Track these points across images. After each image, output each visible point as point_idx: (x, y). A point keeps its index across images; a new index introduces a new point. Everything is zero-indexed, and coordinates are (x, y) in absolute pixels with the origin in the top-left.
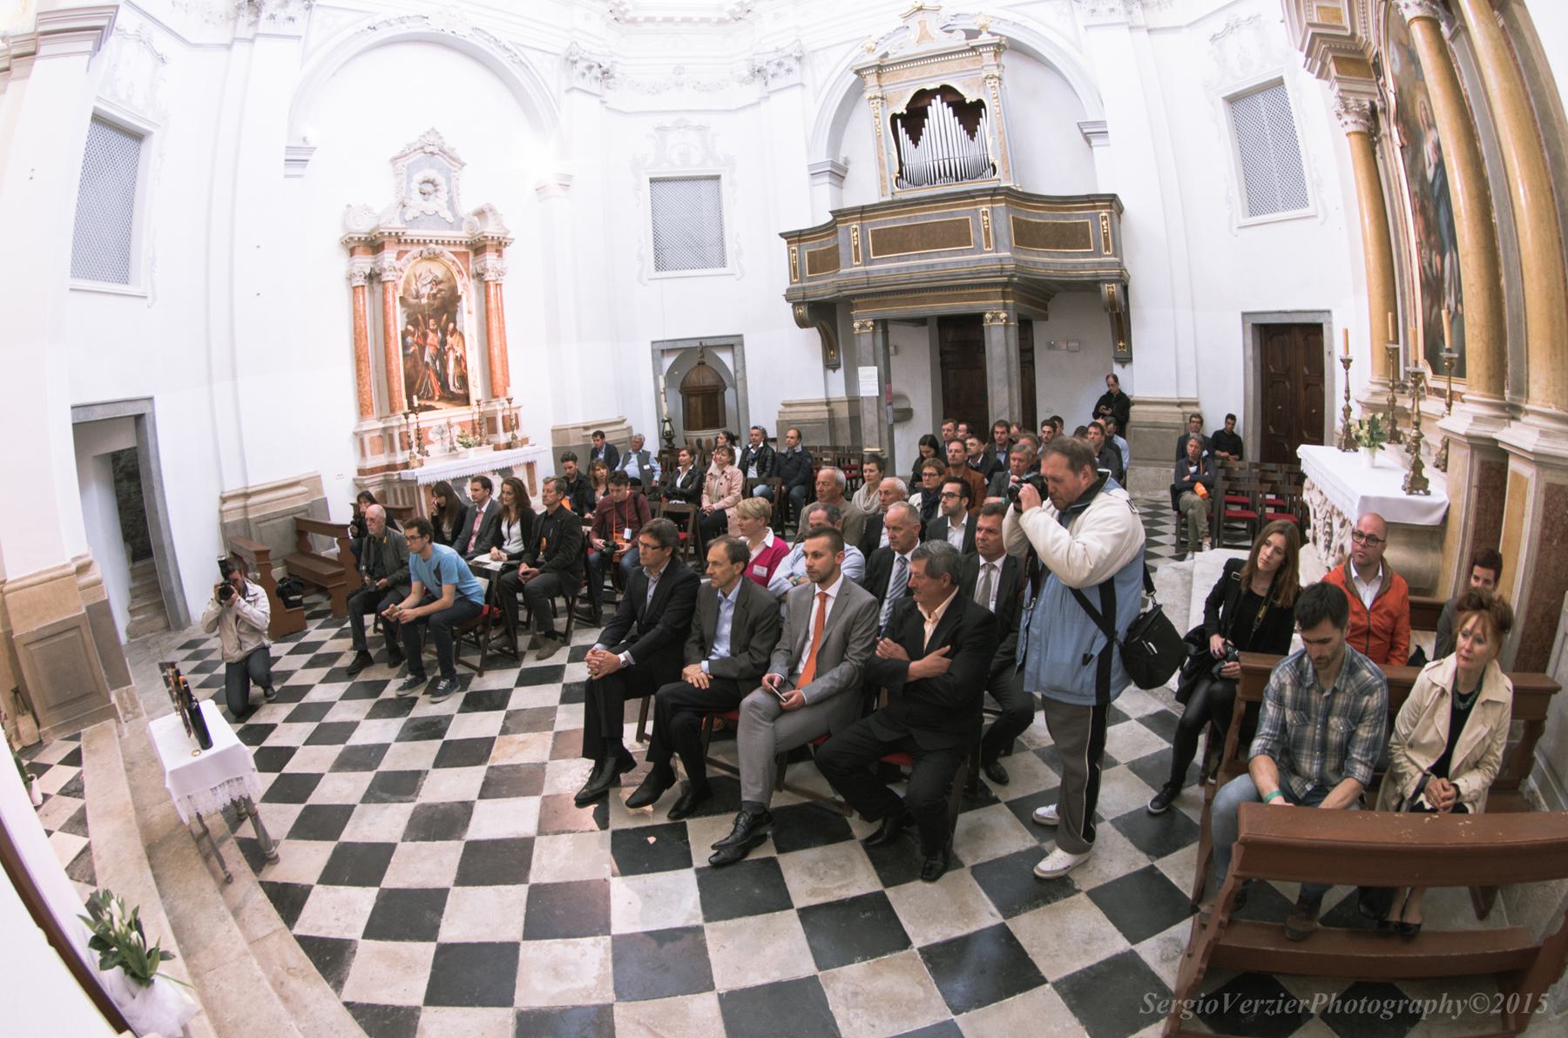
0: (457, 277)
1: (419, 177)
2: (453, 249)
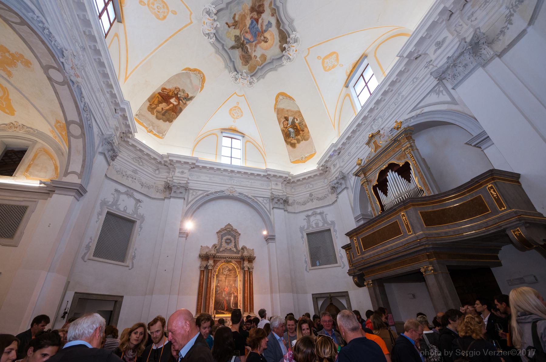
1: (225, 238)
2: (236, 260)
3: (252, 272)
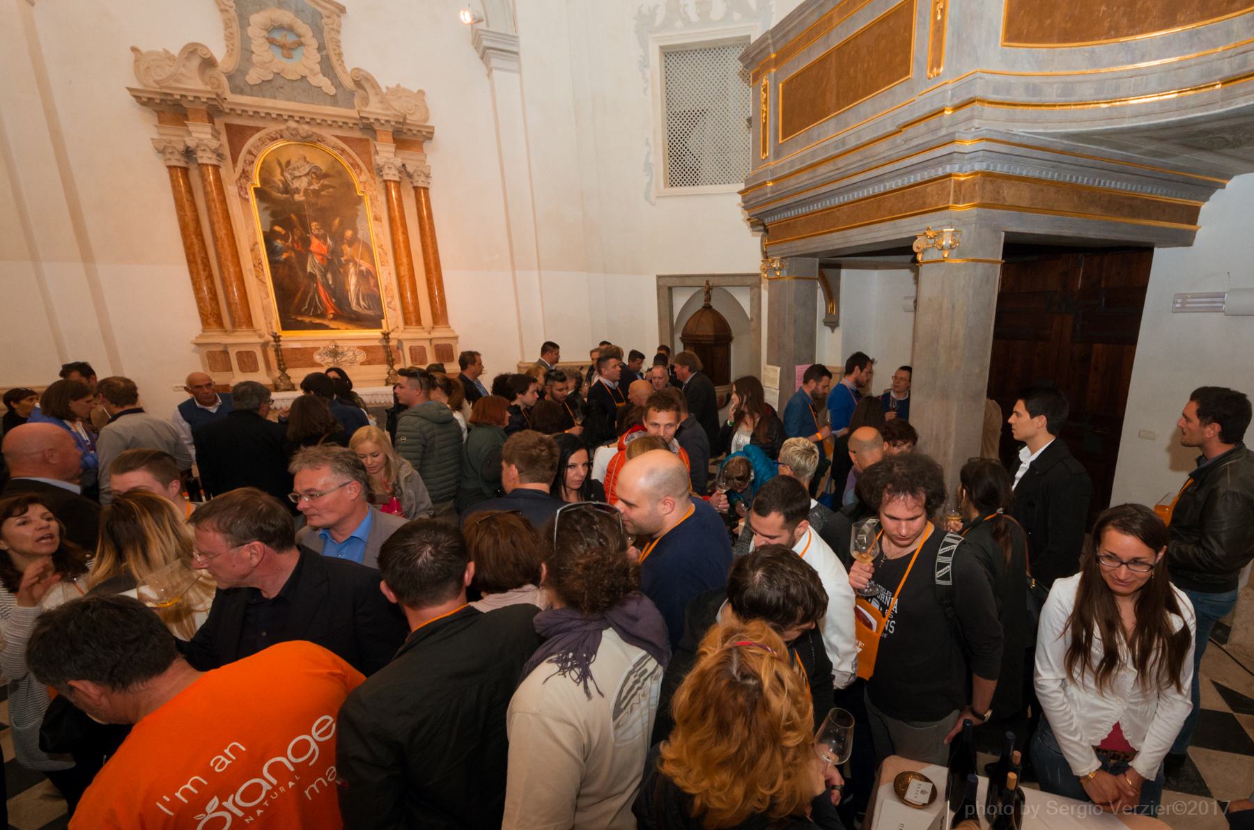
0: (353, 174)
3: (426, 189)
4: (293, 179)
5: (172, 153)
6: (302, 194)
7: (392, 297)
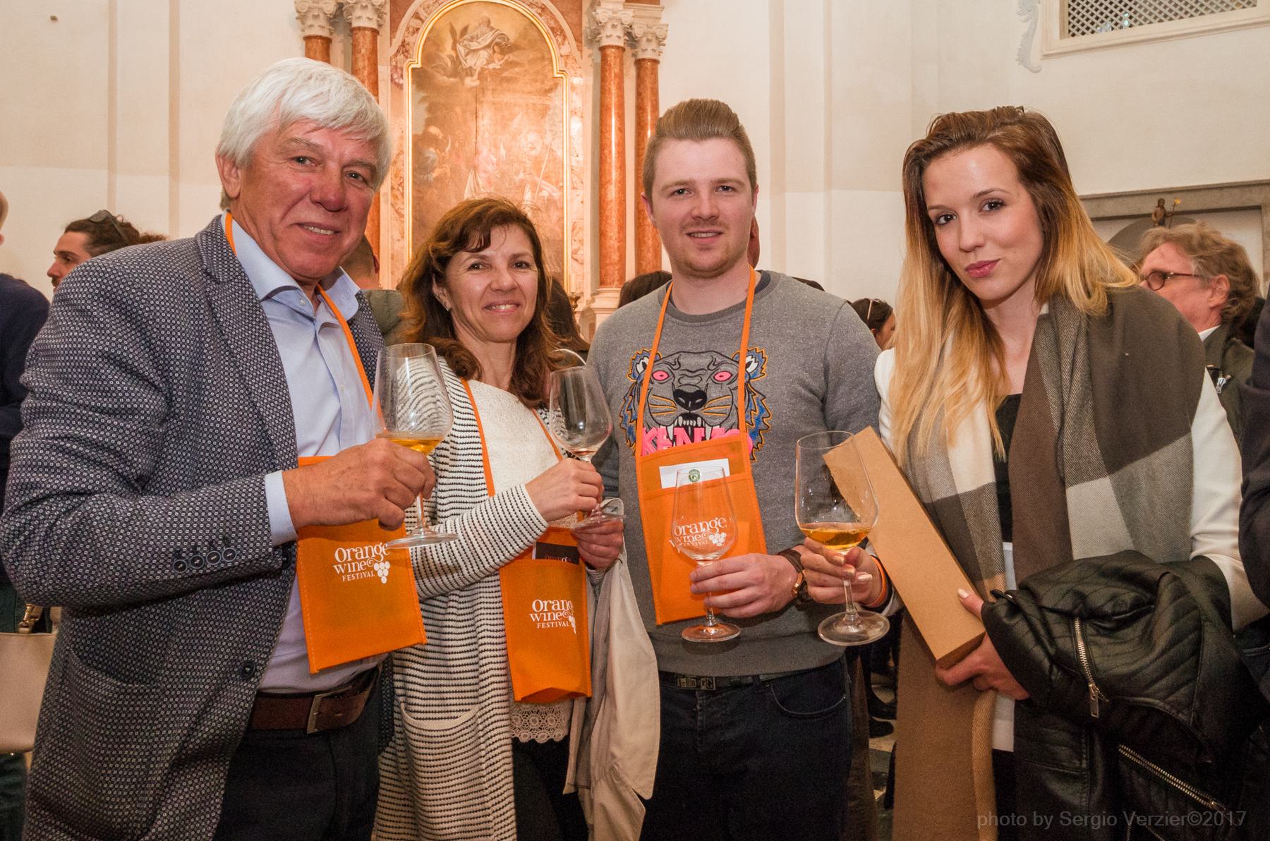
0: (552, 43)
4: (467, 54)
5: (316, 17)
6: (476, 76)
7: (581, 242)
